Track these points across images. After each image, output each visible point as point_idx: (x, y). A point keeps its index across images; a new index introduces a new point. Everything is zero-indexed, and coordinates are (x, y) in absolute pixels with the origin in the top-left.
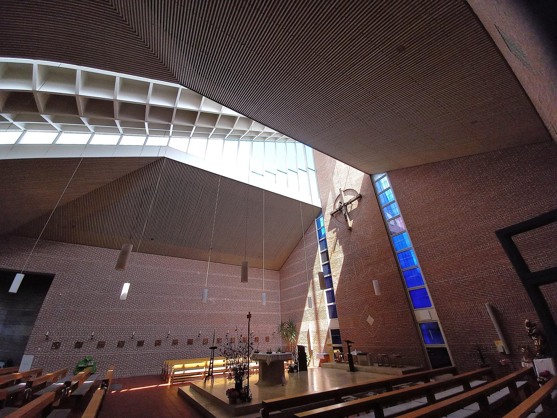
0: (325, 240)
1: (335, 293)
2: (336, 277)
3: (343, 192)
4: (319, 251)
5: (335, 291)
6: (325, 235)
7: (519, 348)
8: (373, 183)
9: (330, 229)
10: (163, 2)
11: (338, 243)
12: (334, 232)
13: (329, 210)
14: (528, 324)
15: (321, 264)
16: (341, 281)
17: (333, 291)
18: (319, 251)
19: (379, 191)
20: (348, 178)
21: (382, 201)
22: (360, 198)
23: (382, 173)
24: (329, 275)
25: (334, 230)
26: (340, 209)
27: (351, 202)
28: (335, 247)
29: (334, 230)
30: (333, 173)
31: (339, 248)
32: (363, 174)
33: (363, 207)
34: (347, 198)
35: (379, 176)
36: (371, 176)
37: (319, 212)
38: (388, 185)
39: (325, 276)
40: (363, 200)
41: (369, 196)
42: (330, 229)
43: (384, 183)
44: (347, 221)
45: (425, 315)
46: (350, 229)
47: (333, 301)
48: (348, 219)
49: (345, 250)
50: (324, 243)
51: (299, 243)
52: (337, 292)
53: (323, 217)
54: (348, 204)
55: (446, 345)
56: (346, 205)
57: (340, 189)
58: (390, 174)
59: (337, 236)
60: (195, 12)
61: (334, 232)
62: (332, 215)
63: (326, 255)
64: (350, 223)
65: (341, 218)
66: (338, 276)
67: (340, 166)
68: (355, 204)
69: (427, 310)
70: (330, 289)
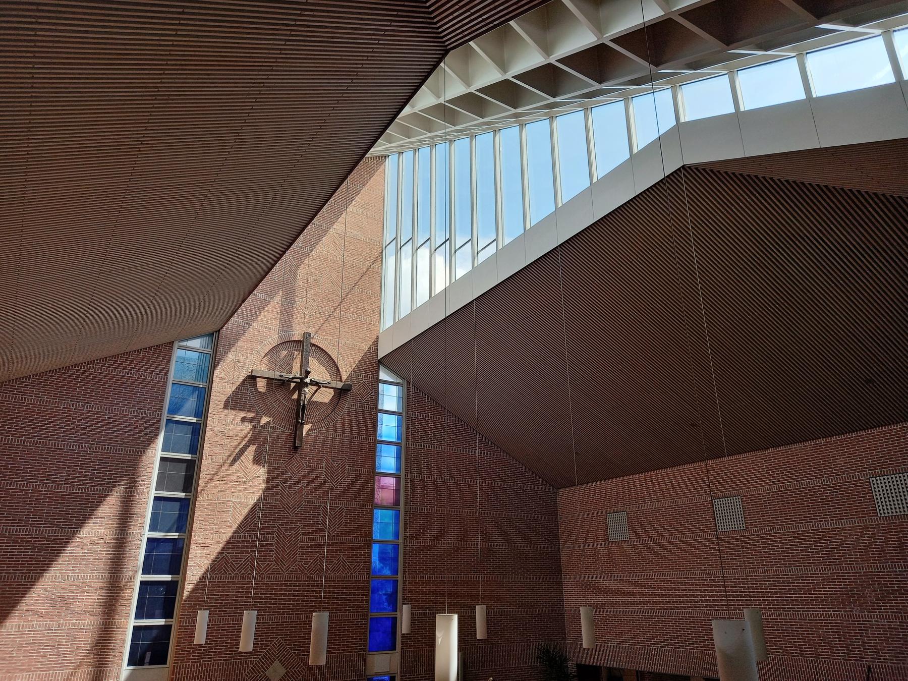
1: (186, 594)
2: (206, 551)
15: (153, 493)
16: (219, 565)
17: (172, 588)
18: (156, 452)
34: (318, 371)
40: (348, 403)
41: (356, 398)
47: (168, 613)
52: (194, 590)
63: (186, 474)
66: (215, 550)
68: (325, 396)
69: (388, 656)
70: (167, 578)
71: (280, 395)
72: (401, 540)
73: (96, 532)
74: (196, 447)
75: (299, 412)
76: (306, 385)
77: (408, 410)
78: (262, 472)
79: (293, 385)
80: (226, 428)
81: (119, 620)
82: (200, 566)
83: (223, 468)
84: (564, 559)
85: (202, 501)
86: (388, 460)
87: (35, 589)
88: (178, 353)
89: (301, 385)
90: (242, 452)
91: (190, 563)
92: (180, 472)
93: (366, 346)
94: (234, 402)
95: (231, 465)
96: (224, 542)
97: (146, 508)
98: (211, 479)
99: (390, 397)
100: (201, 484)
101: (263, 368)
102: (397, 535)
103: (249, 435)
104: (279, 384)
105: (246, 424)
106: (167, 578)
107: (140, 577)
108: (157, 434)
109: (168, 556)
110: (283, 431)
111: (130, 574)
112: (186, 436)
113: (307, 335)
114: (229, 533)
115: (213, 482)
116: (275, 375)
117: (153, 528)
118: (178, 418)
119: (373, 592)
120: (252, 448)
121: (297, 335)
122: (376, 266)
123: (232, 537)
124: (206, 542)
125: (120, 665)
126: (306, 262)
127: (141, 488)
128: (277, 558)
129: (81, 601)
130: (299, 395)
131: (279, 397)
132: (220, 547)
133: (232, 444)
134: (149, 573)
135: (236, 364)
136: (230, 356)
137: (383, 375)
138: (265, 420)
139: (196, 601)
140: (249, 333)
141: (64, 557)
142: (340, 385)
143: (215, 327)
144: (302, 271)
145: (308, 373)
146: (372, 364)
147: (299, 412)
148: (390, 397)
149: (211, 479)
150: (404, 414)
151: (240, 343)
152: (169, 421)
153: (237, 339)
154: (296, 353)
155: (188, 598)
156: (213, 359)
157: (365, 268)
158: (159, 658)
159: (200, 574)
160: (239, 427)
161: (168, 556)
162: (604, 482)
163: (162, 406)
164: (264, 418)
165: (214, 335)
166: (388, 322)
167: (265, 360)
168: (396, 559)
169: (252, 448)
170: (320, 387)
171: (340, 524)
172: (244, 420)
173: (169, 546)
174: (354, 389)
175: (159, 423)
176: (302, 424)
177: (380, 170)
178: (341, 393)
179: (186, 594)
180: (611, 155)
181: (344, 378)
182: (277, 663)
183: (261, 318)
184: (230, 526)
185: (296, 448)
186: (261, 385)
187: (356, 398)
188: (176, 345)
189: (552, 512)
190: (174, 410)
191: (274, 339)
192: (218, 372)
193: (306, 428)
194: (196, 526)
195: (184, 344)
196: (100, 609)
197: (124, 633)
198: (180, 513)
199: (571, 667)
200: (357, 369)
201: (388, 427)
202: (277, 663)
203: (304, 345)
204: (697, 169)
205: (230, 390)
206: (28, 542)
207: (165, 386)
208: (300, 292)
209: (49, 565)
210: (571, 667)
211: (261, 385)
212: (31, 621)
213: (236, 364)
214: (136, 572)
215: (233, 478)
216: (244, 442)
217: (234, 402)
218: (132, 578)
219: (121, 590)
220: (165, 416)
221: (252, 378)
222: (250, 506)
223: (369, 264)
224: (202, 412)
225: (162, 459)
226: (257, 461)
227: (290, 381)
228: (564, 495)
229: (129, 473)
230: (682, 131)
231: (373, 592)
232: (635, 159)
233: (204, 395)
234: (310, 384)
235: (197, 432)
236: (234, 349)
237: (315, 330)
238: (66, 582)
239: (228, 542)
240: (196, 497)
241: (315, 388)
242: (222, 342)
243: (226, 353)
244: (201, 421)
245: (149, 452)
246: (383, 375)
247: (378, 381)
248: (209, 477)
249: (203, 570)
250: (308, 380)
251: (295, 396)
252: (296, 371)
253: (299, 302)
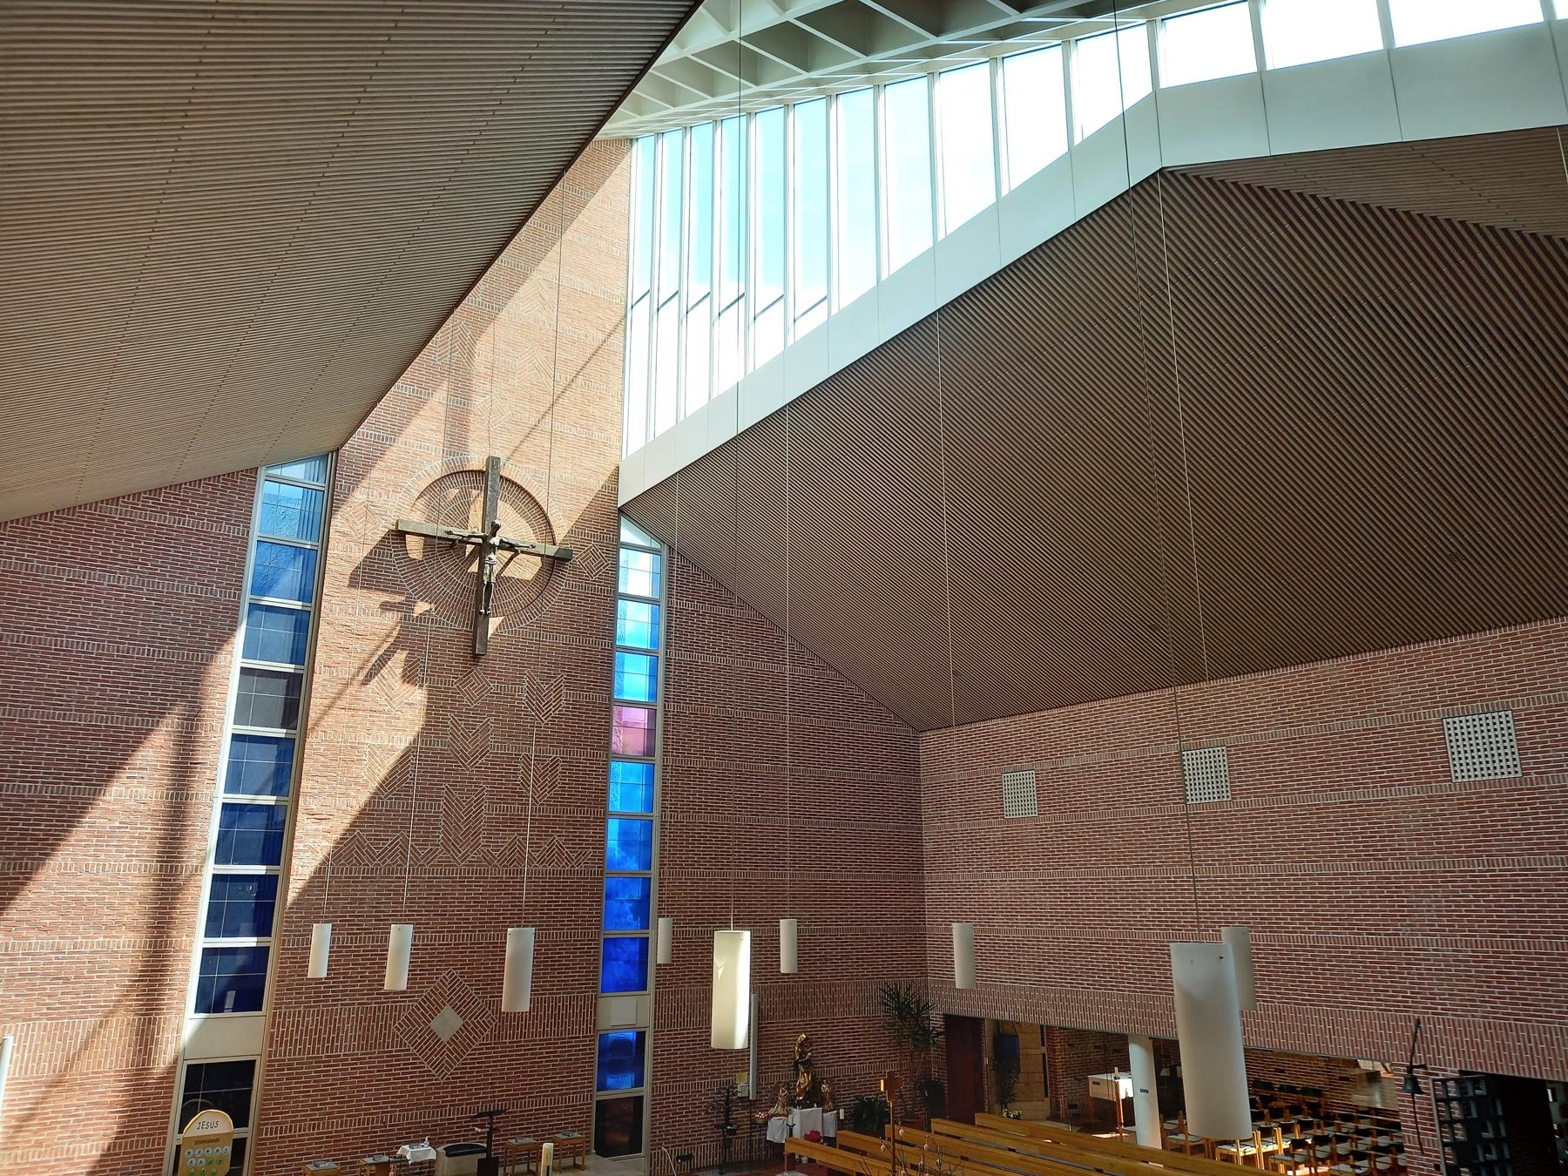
1: (292, 896)
2: (324, 826)
5: (294, 887)
7: (777, 1088)
14: (801, 1045)
16: (346, 850)
17: (268, 886)
18: (233, 658)
23: (654, 535)
34: (513, 526)
40: (565, 582)
45: (624, 1013)
47: (262, 927)
52: (306, 891)
54: (511, 547)
55: (646, 1091)
66: (340, 824)
68: (526, 569)
69: (634, 999)
70: (260, 870)
71: (447, 565)
72: (656, 812)
73: (134, 793)
74: (302, 650)
75: (482, 594)
76: (493, 548)
77: (670, 596)
78: (419, 695)
79: (470, 548)
80: (353, 621)
81: (178, 937)
82: (313, 850)
83: (351, 689)
84: (929, 846)
85: (315, 744)
86: (634, 680)
87: (31, 885)
88: (265, 489)
89: (484, 548)
90: (383, 661)
91: (297, 845)
92: (276, 695)
93: (597, 483)
94: (366, 576)
95: (365, 682)
96: (355, 811)
97: (218, 752)
98: (330, 707)
99: (639, 572)
100: (313, 715)
101: (416, 519)
102: (649, 804)
103: (395, 633)
104: (446, 547)
105: (389, 614)
106: (260, 870)
107: (211, 868)
108: (233, 629)
109: (261, 833)
110: (455, 627)
111: (195, 862)
112: (282, 632)
113: (493, 462)
114: (363, 798)
115: (334, 711)
116: (439, 530)
117: (232, 787)
118: (268, 601)
119: (608, 897)
120: (401, 656)
121: (477, 462)
122: (616, 340)
123: (368, 804)
124: (324, 810)
125: (181, 1011)
126: (490, 330)
127: (209, 720)
129: (111, 906)
130: (481, 567)
131: (446, 569)
132: (348, 820)
133: (364, 648)
134: (227, 863)
135: (368, 508)
136: (359, 496)
137: (628, 534)
138: (421, 607)
139: (309, 909)
140: (391, 455)
141: (79, 834)
142: (551, 550)
143: (329, 444)
144: (482, 348)
145: (496, 528)
146: (610, 514)
147: (482, 594)
148: (639, 572)
149: (330, 707)
150: (663, 604)
151: (374, 474)
152: (254, 607)
153: (369, 466)
154: (475, 492)
155: (296, 902)
156: (329, 501)
157: (596, 344)
158: (249, 999)
159: (316, 864)
160: (377, 619)
161: (261, 833)
162: (999, 721)
163: (240, 580)
164: (420, 603)
165: (330, 457)
166: (635, 440)
167: (421, 504)
168: (647, 844)
169: (401, 656)
170: (517, 554)
171: (553, 786)
172: (385, 607)
173: (261, 819)
174: (577, 558)
175: (236, 609)
176: (487, 616)
177: (623, 165)
178: (555, 563)
179: (292, 896)
180: (1037, 146)
181: (559, 538)
182: (448, 1011)
183: (410, 430)
184: (365, 786)
185: (476, 657)
186: (414, 547)
187: (581, 573)
188: (262, 473)
189: (910, 767)
190: (261, 588)
191: (435, 467)
192: (337, 523)
193: (494, 623)
194: (306, 784)
195: (276, 472)
196: (143, 921)
197: (187, 959)
198: (280, 761)
199: (936, 1020)
201: (636, 624)
202: (448, 1011)
203: (486, 479)
204: (1184, 175)
205: (360, 554)
206: (18, 807)
207: (245, 546)
208: (479, 385)
209: (54, 847)
210: (936, 1020)
211: (414, 547)
212: (27, 938)
213: (368, 508)
214: (204, 860)
215: (368, 705)
216: (386, 646)
217: (366, 576)
218: (197, 870)
219: (180, 888)
220: (247, 597)
221: (399, 535)
222: (398, 754)
223: (602, 337)
224: (311, 591)
225: (245, 671)
226: (409, 677)
227: (464, 541)
228: (931, 740)
229: (187, 690)
230: (1162, 105)
231: (608, 897)
232: (1077, 157)
233: (314, 563)
234: (500, 548)
235: (304, 627)
236: (365, 483)
237: (508, 453)
238: (85, 875)
239: (362, 812)
240: (305, 736)
241: (508, 554)
242: (344, 470)
243: (351, 490)
244: (310, 607)
245: (221, 658)
246: (628, 534)
247: (618, 545)
248: (327, 702)
249: (320, 857)
250: (495, 541)
251: (474, 568)
252: (475, 525)
253: (478, 402)
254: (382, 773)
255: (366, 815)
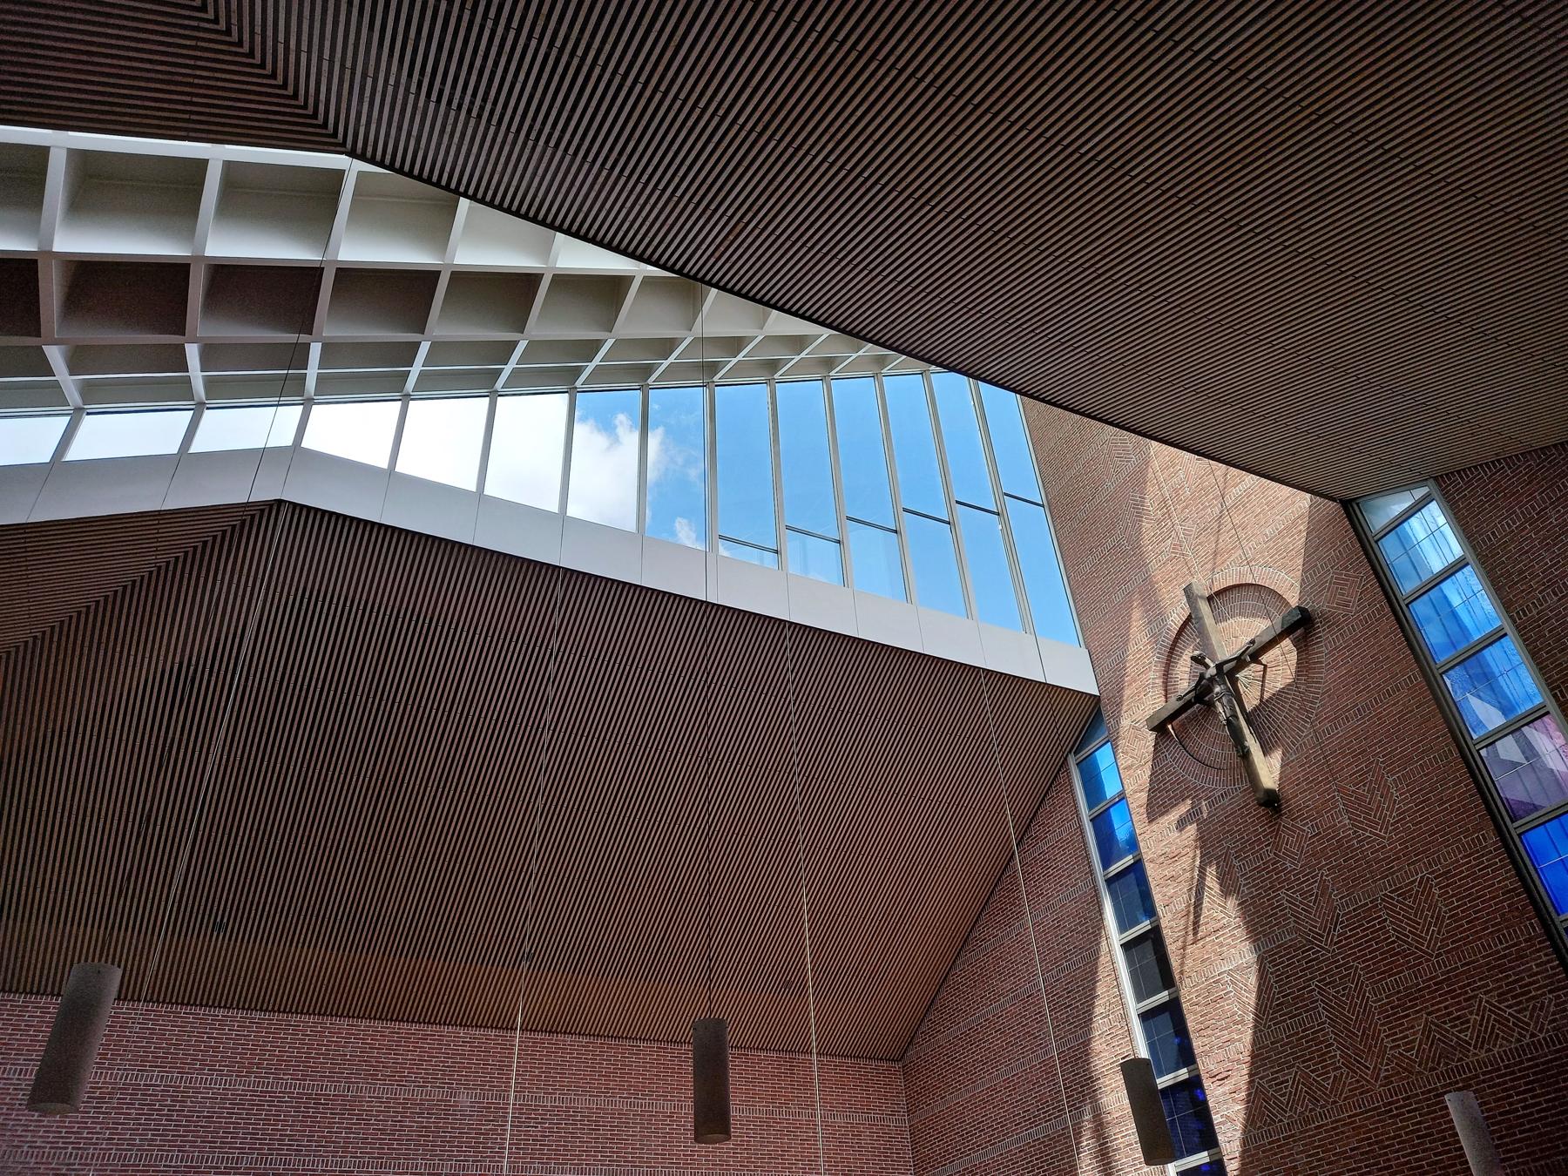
0: (1137, 868)
2: (1228, 1086)
3: (1204, 607)
4: (1114, 937)
6: (1133, 844)
8: (1366, 545)
9: (1155, 810)
10: (295, 7)
11: (1212, 882)
12: (1181, 824)
13: (1143, 703)
15: (1133, 1008)
18: (1114, 937)
19: (1407, 586)
20: (1230, 531)
21: (1433, 635)
22: (1300, 626)
24: (1183, 1074)
25: (1184, 808)
26: (1201, 694)
27: (1254, 654)
28: (1198, 905)
29: (1184, 808)
30: (1138, 511)
31: (1222, 913)
32: (1304, 500)
33: (1327, 676)
34: (1233, 634)
35: (1398, 505)
36: (1350, 507)
37: (1088, 718)
38: (1454, 548)
39: (1163, 1082)
40: (1326, 642)
42: (1155, 810)
43: (1430, 537)
44: (1245, 755)
46: (1271, 802)
48: (1252, 743)
49: (1259, 923)
50: (1133, 888)
51: (994, 893)
53: (1113, 741)
54: (1240, 662)
56: (1229, 672)
57: (1188, 591)
58: (1458, 490)
59: (1203, 841)
60: (515, 25)
61: (1181, 824)
62: (1160, 729)
64: (1269, 770)
65: (1212, 745)
66: (1241, 1076)
67: (1173, 470)
68: (1282, 663)
70: (1202, 1158)
85: (1189, 995)
98: (1184, 948)
114: (1248, 1037)
123: (1254, 1043)
128: (1345, 1056)
151: (1127, 692)
171: (1439, 919)
175: (1096, 889)
184: (1242, 1022)
200: (1309, 567)
225: (1126, 947)
237: (1209, 566)
239: (1253, 1056)
248: (1180, 944)
249: (1239, 1126)
254: (1251, 999)
255: (1259, 1058)
